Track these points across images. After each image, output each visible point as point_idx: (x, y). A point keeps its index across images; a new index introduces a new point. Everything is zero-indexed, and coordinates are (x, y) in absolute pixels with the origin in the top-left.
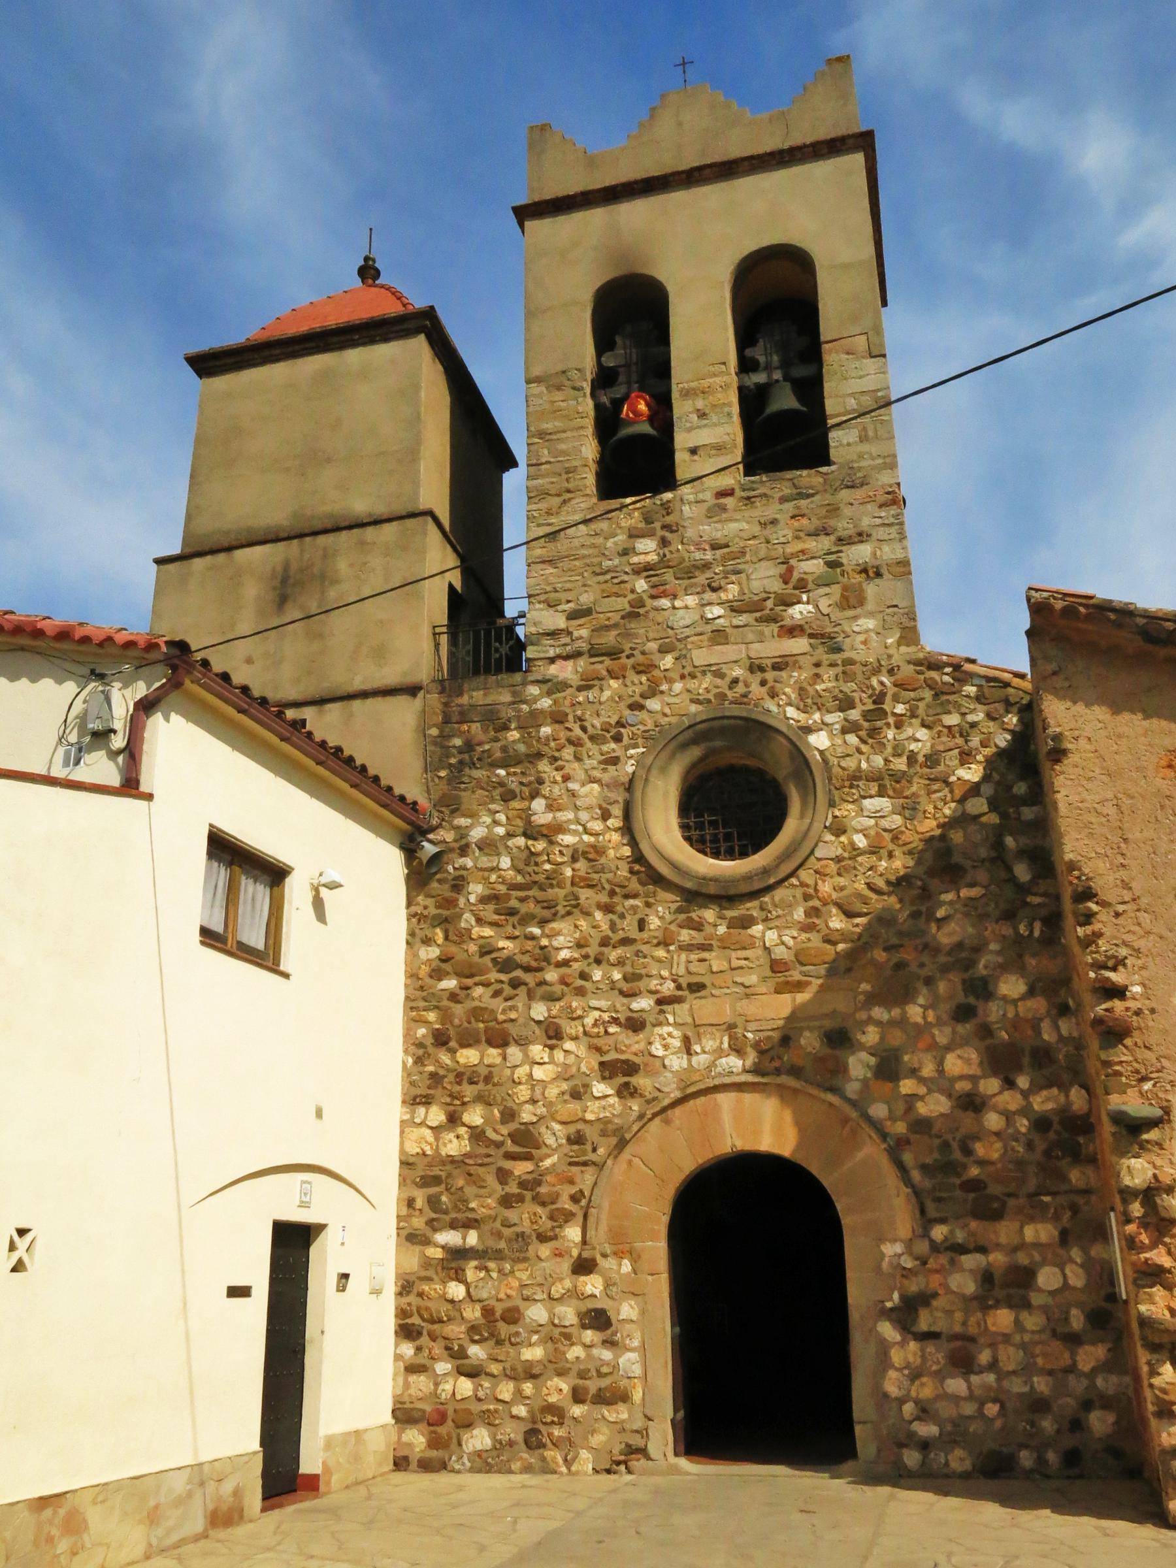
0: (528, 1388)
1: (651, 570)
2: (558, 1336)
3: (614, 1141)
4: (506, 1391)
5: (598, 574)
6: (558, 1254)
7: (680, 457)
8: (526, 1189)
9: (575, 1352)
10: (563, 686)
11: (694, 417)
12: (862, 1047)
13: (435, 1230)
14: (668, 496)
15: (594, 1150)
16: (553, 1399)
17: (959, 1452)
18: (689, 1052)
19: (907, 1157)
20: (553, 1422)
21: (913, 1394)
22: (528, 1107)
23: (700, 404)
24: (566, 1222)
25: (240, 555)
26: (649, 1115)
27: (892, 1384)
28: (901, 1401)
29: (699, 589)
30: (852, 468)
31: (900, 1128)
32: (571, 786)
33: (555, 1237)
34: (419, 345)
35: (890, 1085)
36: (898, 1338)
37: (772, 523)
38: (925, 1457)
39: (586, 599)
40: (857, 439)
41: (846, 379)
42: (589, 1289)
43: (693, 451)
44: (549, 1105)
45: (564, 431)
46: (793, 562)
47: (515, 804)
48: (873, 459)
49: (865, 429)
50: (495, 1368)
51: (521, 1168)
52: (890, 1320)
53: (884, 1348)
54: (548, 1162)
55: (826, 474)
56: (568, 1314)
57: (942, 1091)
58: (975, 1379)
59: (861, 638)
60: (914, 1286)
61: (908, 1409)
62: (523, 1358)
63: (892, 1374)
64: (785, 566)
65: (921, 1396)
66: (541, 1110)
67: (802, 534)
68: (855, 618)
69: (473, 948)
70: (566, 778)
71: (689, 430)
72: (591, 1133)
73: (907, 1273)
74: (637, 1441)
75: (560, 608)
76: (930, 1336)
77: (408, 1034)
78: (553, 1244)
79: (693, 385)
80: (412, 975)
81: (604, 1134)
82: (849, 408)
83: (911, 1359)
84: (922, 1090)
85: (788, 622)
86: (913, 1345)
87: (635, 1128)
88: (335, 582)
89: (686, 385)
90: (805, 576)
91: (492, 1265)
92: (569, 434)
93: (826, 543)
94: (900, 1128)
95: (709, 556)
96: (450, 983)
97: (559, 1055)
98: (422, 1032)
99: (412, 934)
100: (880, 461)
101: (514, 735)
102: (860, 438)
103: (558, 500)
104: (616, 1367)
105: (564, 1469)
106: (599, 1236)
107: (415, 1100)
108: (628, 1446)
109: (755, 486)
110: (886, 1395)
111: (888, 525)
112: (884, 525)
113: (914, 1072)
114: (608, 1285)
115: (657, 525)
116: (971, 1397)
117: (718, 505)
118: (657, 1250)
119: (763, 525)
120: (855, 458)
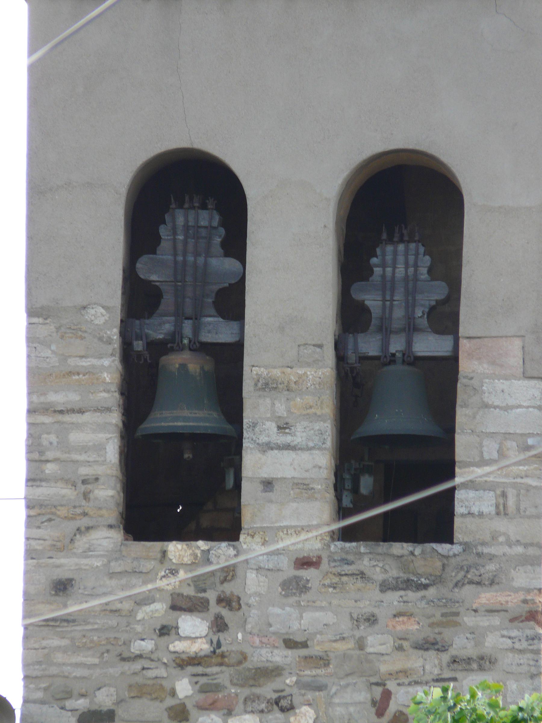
1: (199, 664)
5: (124, 659)
11: (272, 426)
23: (281, 409)
29: (263, 706)
37: (368, 620)
40: (493, 510)
45: (81, 411)
46: (391, 685)
48: (509, 544)
49: (504, 495)
55: (447, 557)
64: (380, 689)
67: (406, 644)
71: (268, 447)
75: (70, 704)
79: (277, 372)
92: (87, 417)
100: (520, 550)
102: (497, 506)
103: (72, 526)
109: (351, 557)
111: (521, 651)
112: (513, 650)
115: (211, 596)
117: (297, 579)
119: (357, 621)
120: (488, 538)
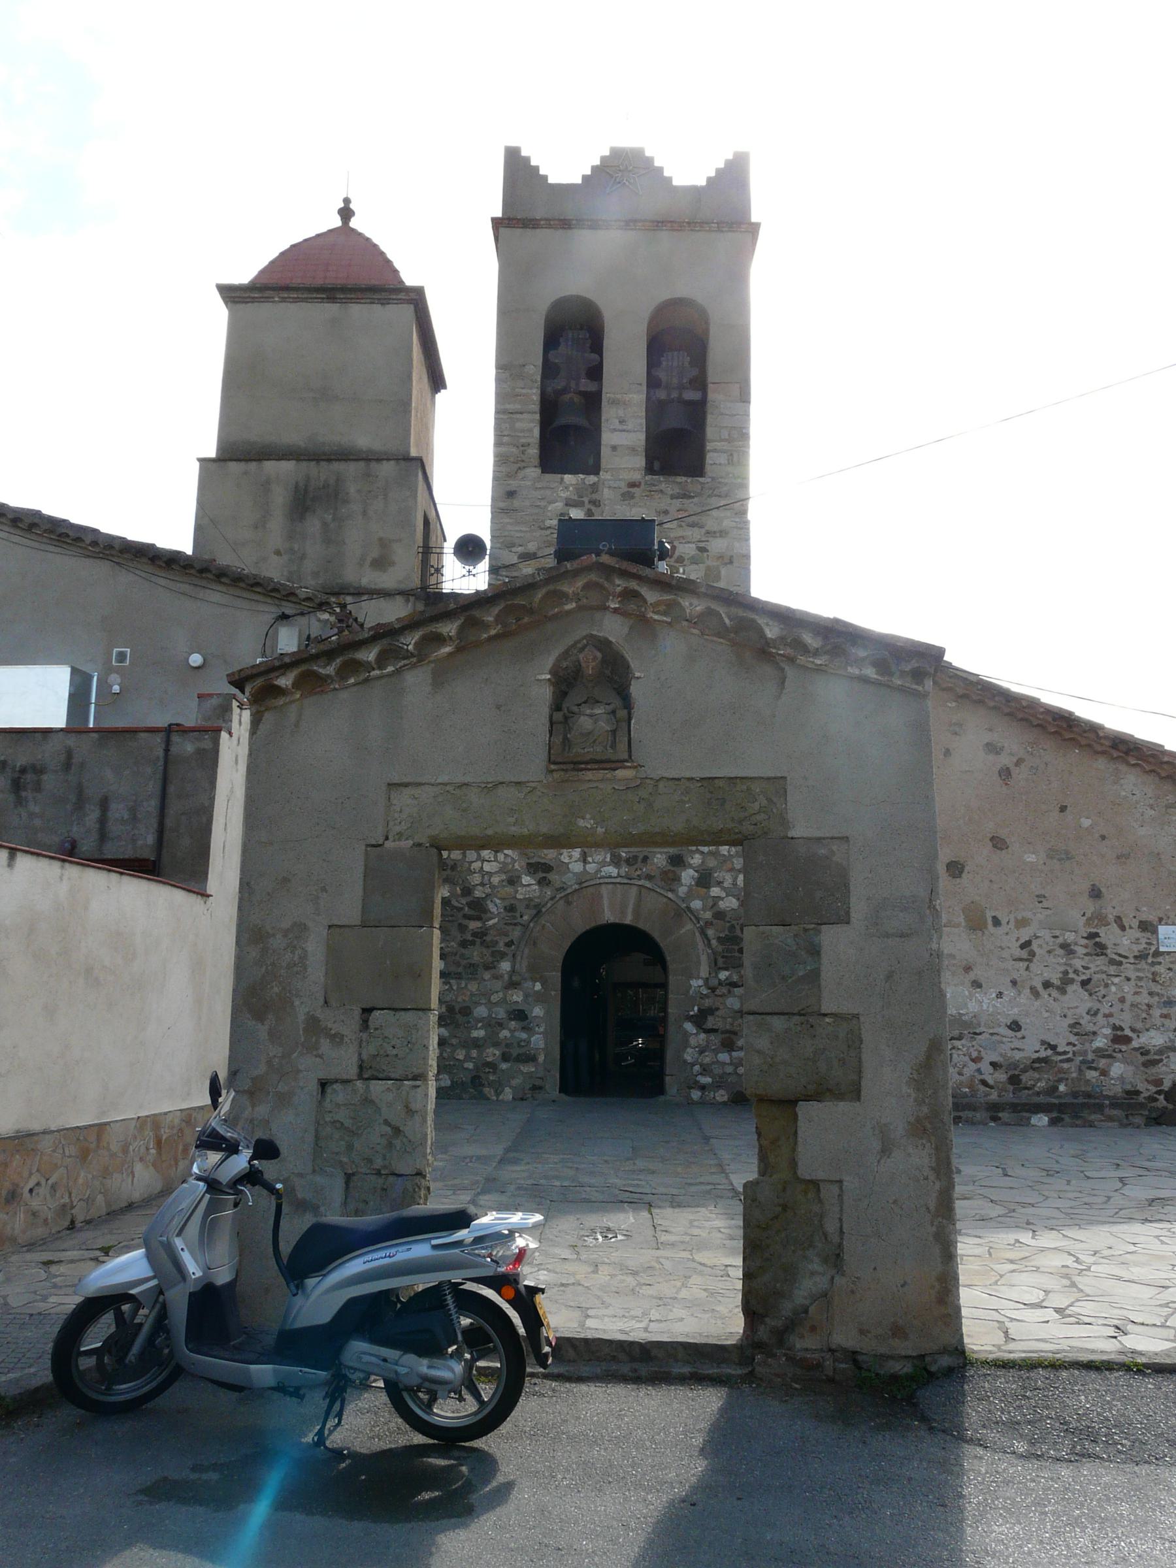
0: (474, 1053)
2: (493, 1025)
3: (534, 912)
4: (460, 1055)
5: (542, 529)
6: (497, 977)
7: (605, 451)
8: (477, 937)
9: (505, 1033)
12: (690, 866)
14: (592, 479)
15: (521, 917)
16: (489, 1059)
17: (722, 1092)
18: (585, 861)
19: (710, 932)
20: (489, 1072)
21: (700, 1061)
22: (480, 888)
23: (621, 413)
24: (502, 958)
25: (270, 466)
26: (558, 896)
27: (689, 1055)
28: (693, 1065)
30: (719, 483)
31: (708, 915)
33: (495, 967)
34: (408, 311)
35: (705, 890)
36: (695, 1031)
38: (703, 1094)
39: (532, 547)
40: (726, 462)
41: (722, 414)
42: (515, 998)
43: (614, 448)
44: (493, 887)
45: (521, 413)
46: (676, 543)
50: (454, 1041)
51: (474, 925)
52: (691, 1022)
53: (686, 1035)
54: (491, 923)
56: (501, 1013)
57: (734, 896)
58: (734, 1054)
60: (707, 1003)
61: (697, 1068)
62: (472, 1036)
63: (689, 1050)
65: (705, 1062)
66: (488, 891)
72: (521, 908)
73: (703, 997)
74: (538, 1083)
75: (514, 549)
76: (708, 1031)
78: (493, 971)
79: (619, 396)
81: (528, 907)
82: (723, 437)
83: (701, 1042)
84: (723, 895)
86: (703, 1036)
87: (549, 905)
88: (346, 501)
89: (612, 396)
90: (683, 555)
91: (453, 982)
92: (525, 416)
93: (696, 534)
94: (708, 915)
97: (501, 857)
102: (728, 460)
104: (529, 1042)
105: (495, 1098)
106: (523, 966)
108: (534, 1085)
109: (656, 483)
110: (685, 1061)
113: (719, 883)
114: (526, 996)
115: (586, 500)
116: (731, 1064)
118: (556, 976)
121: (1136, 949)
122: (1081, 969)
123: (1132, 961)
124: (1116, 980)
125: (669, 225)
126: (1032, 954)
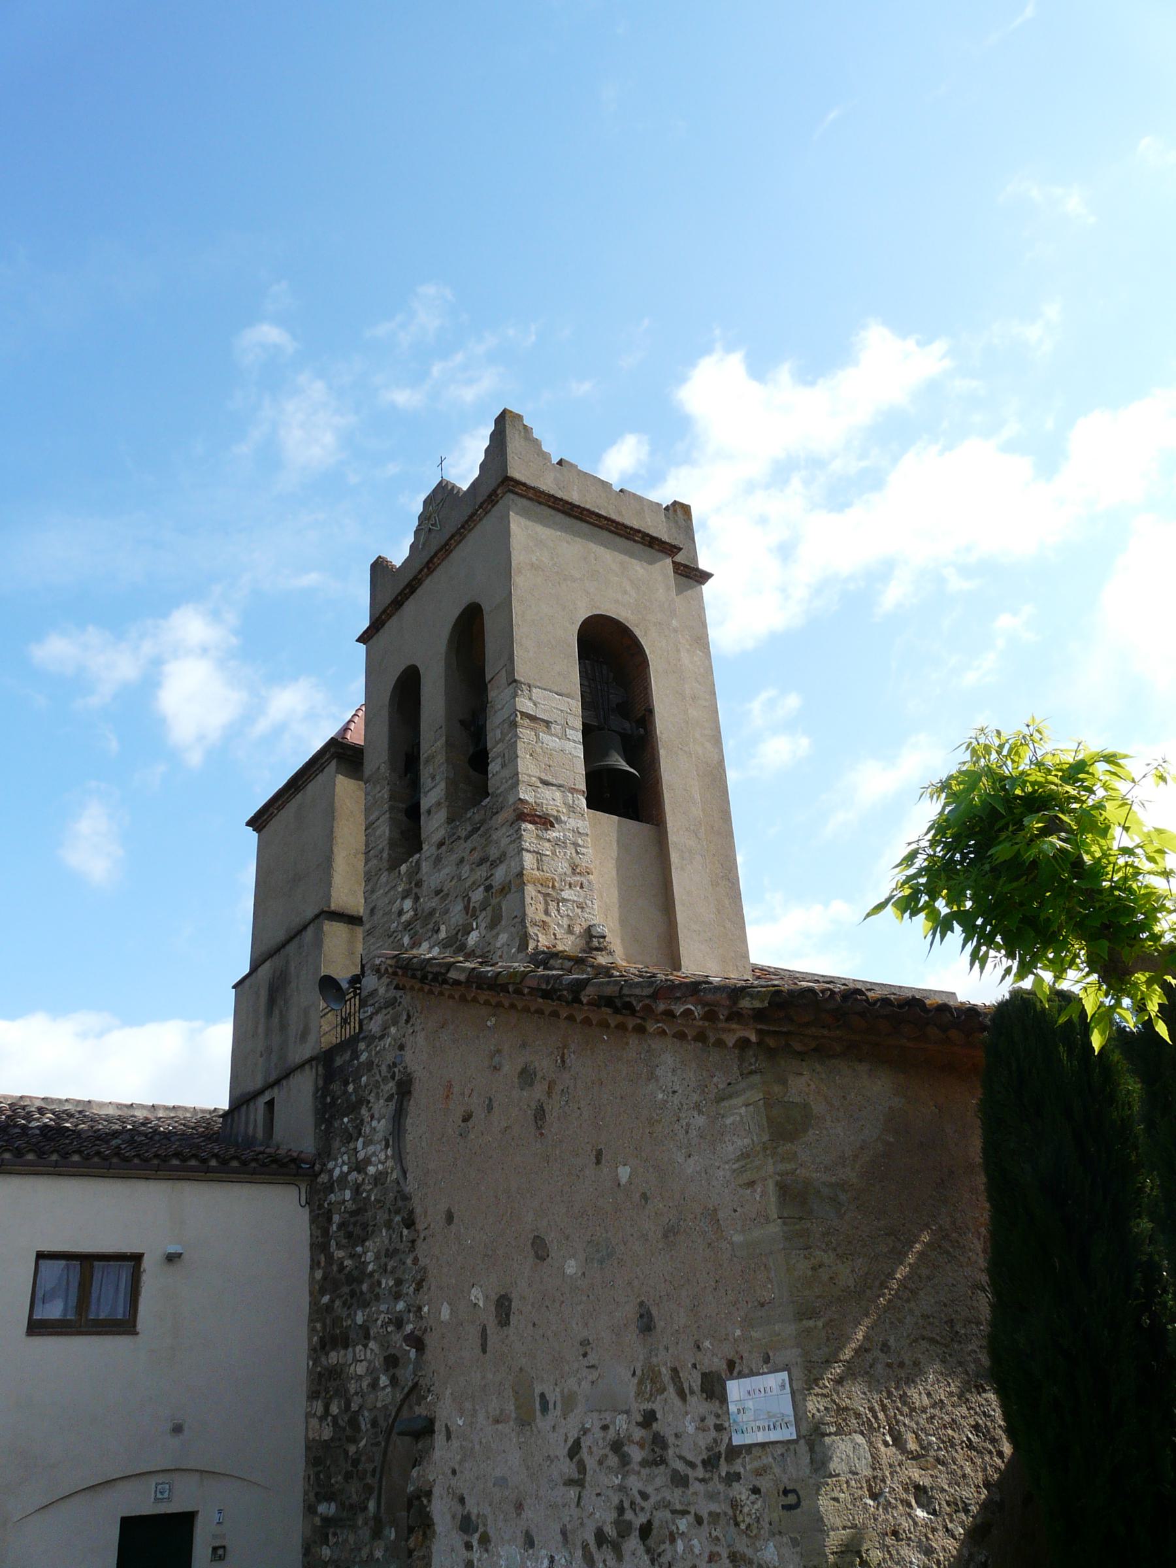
10: (373, 1037)
13: (319, 1502)
32: (374, 1123)
43: (429, 812)
47: (352, 1146)
51: (352, 1449)
59: (499, 953)
68: (498, 934)
69: (335, 1268)
70: (372, 1117)
77: (310, 1339)
80: (311, 1294)
85: (468, 950)
93: (482, 872)
95: (434, 903)
96: (326, 1299)
98: (315, 1339)
99: (312, 1260)
101: (351, 1088)
107: (313, 1396)
115: (413, 885)
121: (704, 1440)
122: (638, 1500)
123: (700, 1472)
124: (683, 1524)
125: (453, 541)
126: (582, 1468)
